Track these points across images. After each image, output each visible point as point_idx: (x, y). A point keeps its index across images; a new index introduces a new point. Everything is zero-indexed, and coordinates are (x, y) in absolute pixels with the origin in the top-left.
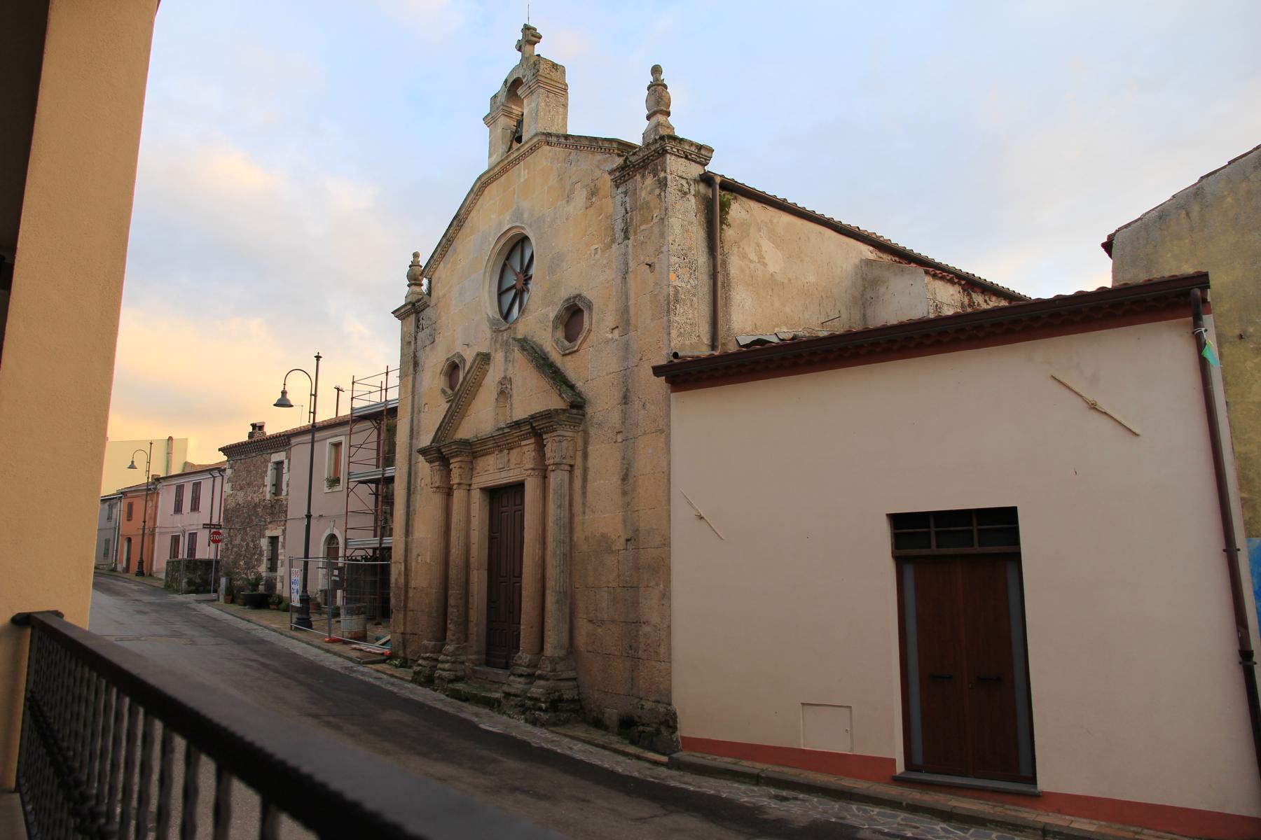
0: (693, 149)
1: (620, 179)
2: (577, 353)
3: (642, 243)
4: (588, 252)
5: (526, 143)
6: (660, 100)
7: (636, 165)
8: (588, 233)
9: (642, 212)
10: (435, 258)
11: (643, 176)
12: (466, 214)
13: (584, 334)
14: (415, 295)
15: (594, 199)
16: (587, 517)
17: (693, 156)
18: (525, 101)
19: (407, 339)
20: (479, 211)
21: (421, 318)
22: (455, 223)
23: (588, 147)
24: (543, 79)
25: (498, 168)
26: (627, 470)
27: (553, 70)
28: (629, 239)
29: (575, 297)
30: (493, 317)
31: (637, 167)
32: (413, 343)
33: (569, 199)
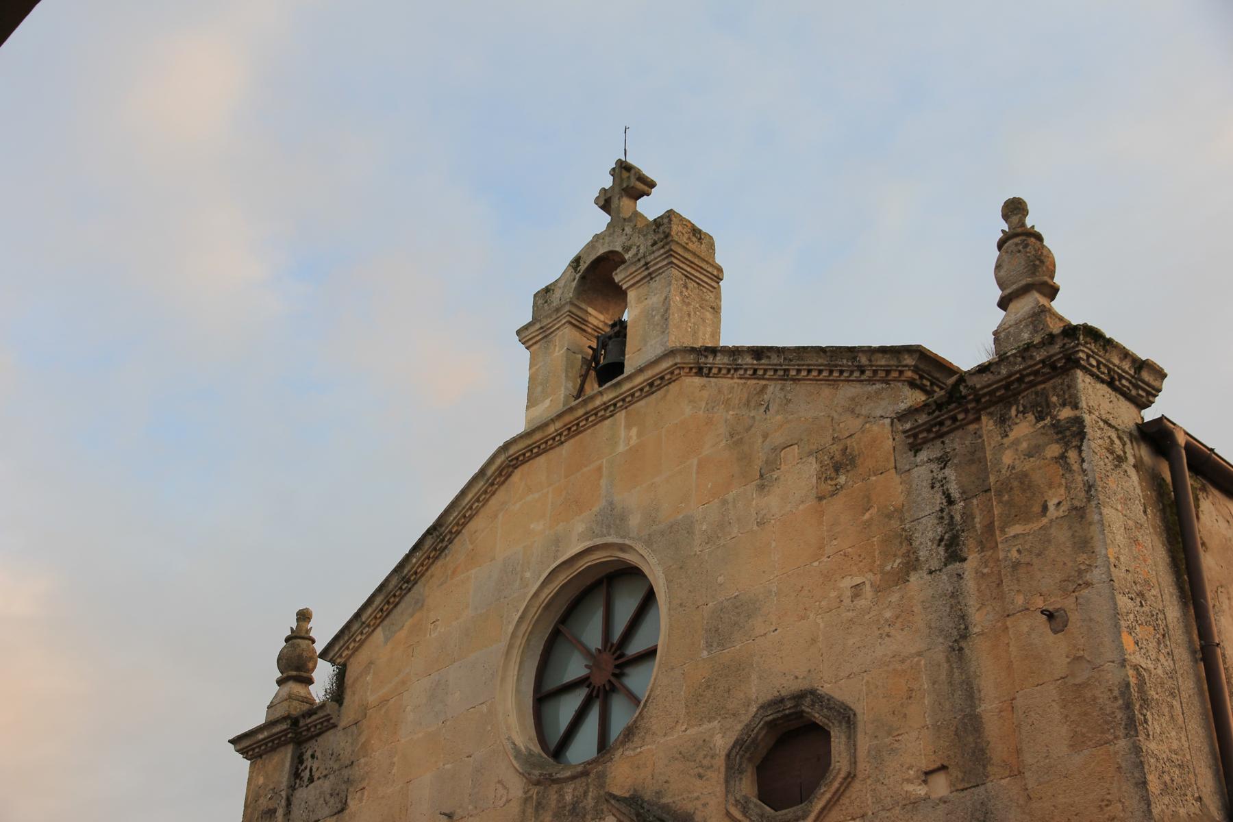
0: (1126, 365)
1: (929, 431)
3: (1016, 566)
4: (833, 594)
5: (630, 377)
6: (1037, 263)
7: (984, 395)
8: (829, 550)
9: (1006, 497)
10: (364, 618)
11: (1003, 420)
13: (836, 785)
14: (295, 703)
15: (842, 479)
17: (1124, 382)
18: (632, 295)
19: (264, 803)
20: (496, 516)
21: (309, 753)
22: (429, 542)
23: (820, 372)
24: (680, 251)
25: (558, 425)
27: (694, 239)
28: (964, 560)
29: (800, 696)
30: (527, 748)
32: (280, 813)
33: (764, 482)
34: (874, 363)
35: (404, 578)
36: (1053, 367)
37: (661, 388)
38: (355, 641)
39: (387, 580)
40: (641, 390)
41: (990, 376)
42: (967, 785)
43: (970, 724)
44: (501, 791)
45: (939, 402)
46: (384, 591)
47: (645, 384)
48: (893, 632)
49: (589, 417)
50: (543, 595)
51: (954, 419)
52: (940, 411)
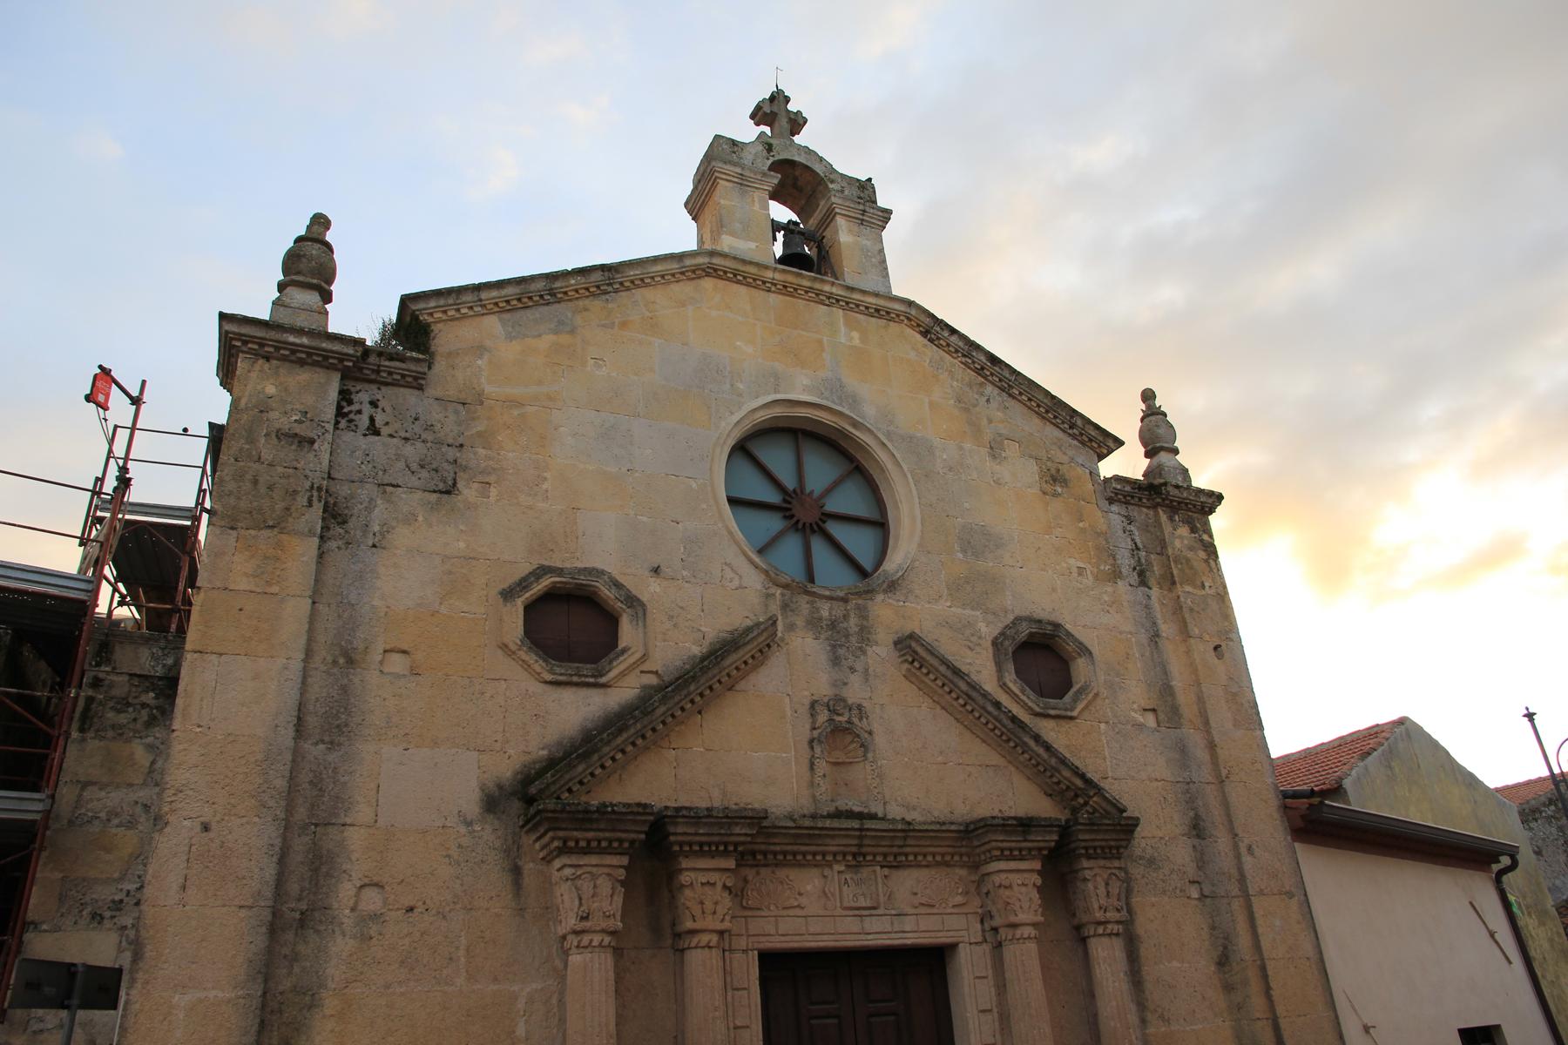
1: (1125, 497)
2: (1072, 723)
10: (484, 295)
12: (632, 282)
16: (1151, 1030)
22: (596, 277)
26: (1225, 948)
31: (1167, 502)
35: (552, 289)
36: (1203, 508)
38: (458, 310)
39: (533, 278)
40: (867, 308)
42: (1171, 726)
43: (1167, 691)
44: (729, 574)
46: (523, 286)
48: (1111, 611)
51: (1140, 499)
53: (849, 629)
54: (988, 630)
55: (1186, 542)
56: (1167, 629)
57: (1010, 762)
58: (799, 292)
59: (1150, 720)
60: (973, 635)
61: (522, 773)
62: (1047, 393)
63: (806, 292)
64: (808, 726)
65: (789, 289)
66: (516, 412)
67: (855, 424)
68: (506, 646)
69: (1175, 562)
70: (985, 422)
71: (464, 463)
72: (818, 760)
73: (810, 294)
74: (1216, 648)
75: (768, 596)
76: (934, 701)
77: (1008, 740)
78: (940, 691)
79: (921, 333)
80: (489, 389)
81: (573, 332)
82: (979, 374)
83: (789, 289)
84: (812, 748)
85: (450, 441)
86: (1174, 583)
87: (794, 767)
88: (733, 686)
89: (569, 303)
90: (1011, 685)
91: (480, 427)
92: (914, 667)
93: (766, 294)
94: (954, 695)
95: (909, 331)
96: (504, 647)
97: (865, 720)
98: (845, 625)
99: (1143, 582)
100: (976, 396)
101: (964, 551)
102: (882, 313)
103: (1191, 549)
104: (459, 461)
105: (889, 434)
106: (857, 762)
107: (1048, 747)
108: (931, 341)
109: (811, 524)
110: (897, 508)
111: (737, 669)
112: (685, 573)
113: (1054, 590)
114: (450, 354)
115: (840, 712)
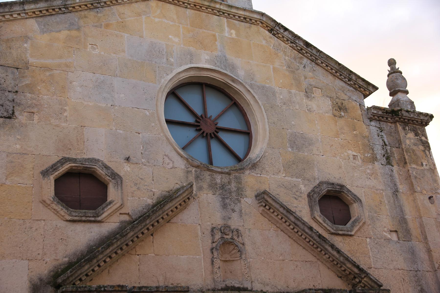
1: (378, 117)
2: (351, 238)
31: (401, 120)
34: (357, 81)
35: (66, 5)
36: (422, 123)
37: (247, 23)
38: (11, 15)
40: (239, 17)
41: (408, 114)
42: (405, 240)
43: (403, 221)
44: (167, 160)
45: (387, 111)
47: (243, 16)
48: (371, 178)
49: (209, 8)
50: (182, 75)
51: (387, 118)
52: (386, 114)
53: (231, 189)
54: (305, 189)
55: (412, 141)
56: (402, 188)
57: (318, 259)
58: (203, 8)
59: (394, 237)
60: (297, 192)
61: (53, 271)
62: (336, 62)
63: (207, 8)
64: (210, 241)
65: (197, 7)
66: (48, 74)
67: (234, 80)
68: (44, 201)
69: (406, 152)
70: (303, 78)
71: (18, 101)
72: (216, 259)
73: (209, 10)
74: (430, 198)
75: (188, 172)
76: (277, 227)
77: (317, 247)
78: (280, 221)
79: (268, 30)
80: (31, 60)
81: (78, 29)
82: (300, 53)
83: (197, 7)
84: (213, 253)
85: (10, 89)
86: (406, 163)
87: (203, 264)
88: (170, 220)
89: (77, 14)
90: (318, 218)
91: (27, 81)
92: (266, 209)
93: (185, 9)
94: (287, 224)
95: (262, 29)
96: (43, 202)
97: (240, 237)
98: (229, 187)
99: (389, 163)
100: (298, 64)
101: (292, 148)
102: (247, 20)
103: (415, 145)
104: (15, 100)
105: (251, 86)
106: (236, 260)
107: (339, 251)
108: (274, 35)
109: (210, 134)
110: (256, 124)
111: (172, 211)
112: (143, 160)
113: (340, 167)
114: (8, 40)
115: (227, 233)
